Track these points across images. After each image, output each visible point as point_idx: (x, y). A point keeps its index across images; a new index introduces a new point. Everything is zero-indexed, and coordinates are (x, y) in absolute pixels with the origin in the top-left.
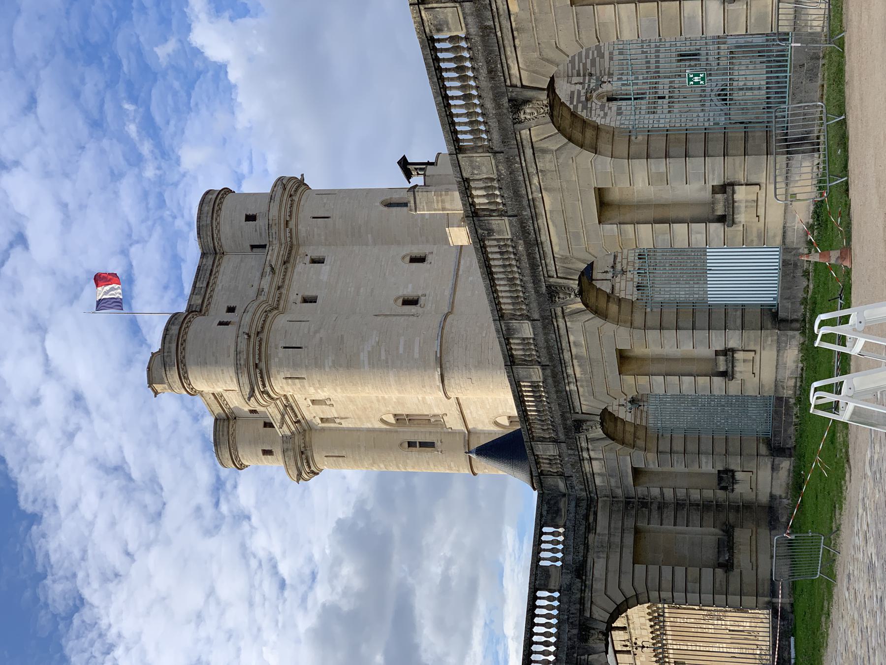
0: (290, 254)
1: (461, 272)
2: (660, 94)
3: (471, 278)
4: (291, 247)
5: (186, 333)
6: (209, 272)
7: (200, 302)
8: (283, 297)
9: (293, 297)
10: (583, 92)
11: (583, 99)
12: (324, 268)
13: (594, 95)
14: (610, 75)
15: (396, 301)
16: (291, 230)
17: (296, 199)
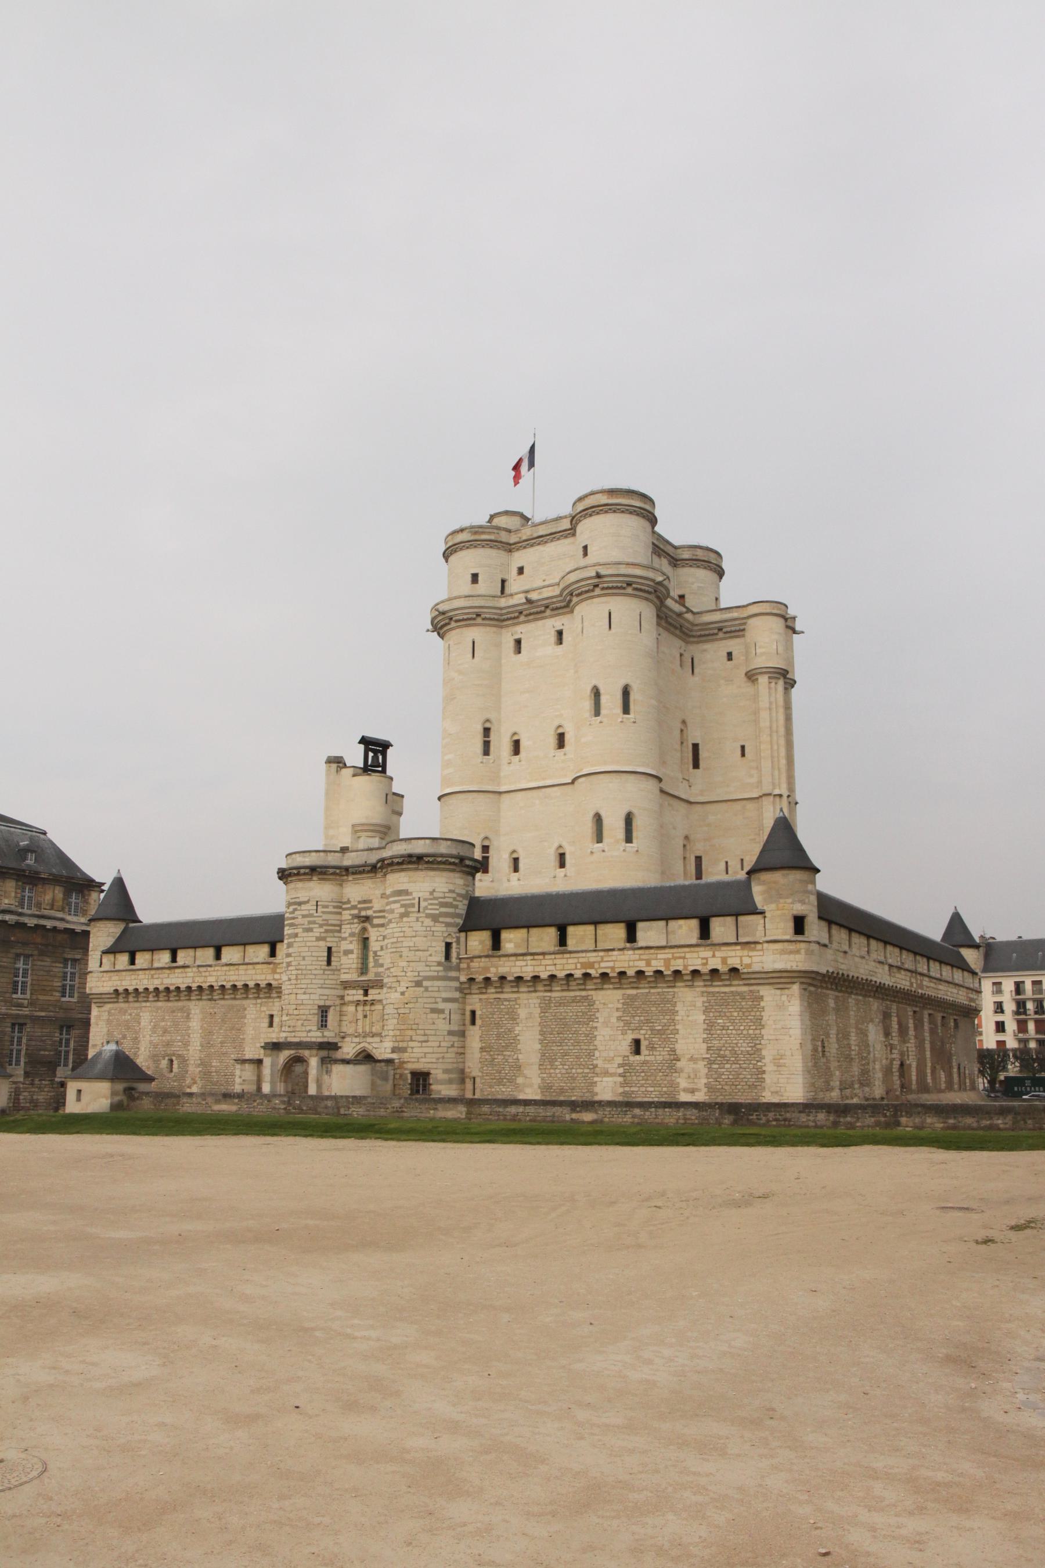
0: (557, 609)
1: (544, 790)
2: (370, 991)
3: (537, 802)
4: (567, 606)
5: (461, 549)
6: (553, 530)
7: (524, 538)
8: (516, 621)
9: (519, 629)
10: (369, 913)
11: (363, 913)
12: (551, 649)
13: (367, 925)
14: (384, 937)
15: (515, 734)
16: (570, 601)
17: (598, 591)
